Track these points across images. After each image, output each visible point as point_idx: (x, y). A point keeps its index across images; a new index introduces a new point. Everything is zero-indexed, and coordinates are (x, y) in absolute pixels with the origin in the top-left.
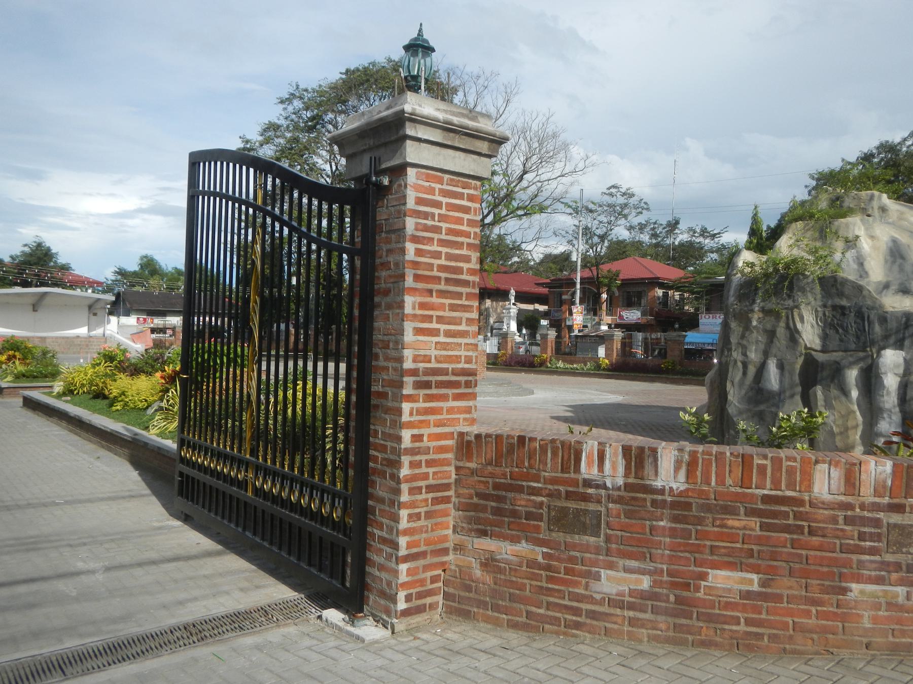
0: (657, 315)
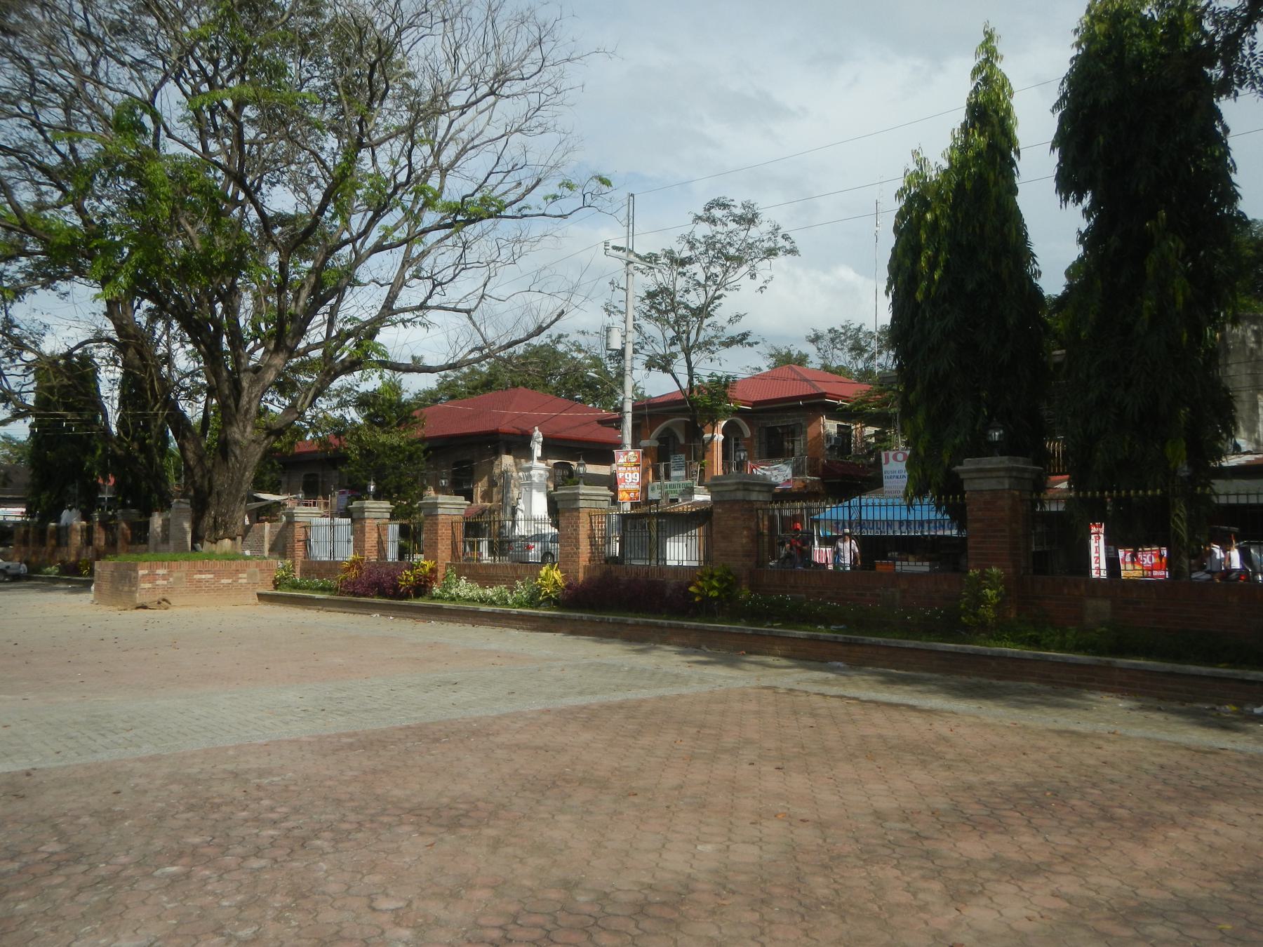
0: (826, 473)
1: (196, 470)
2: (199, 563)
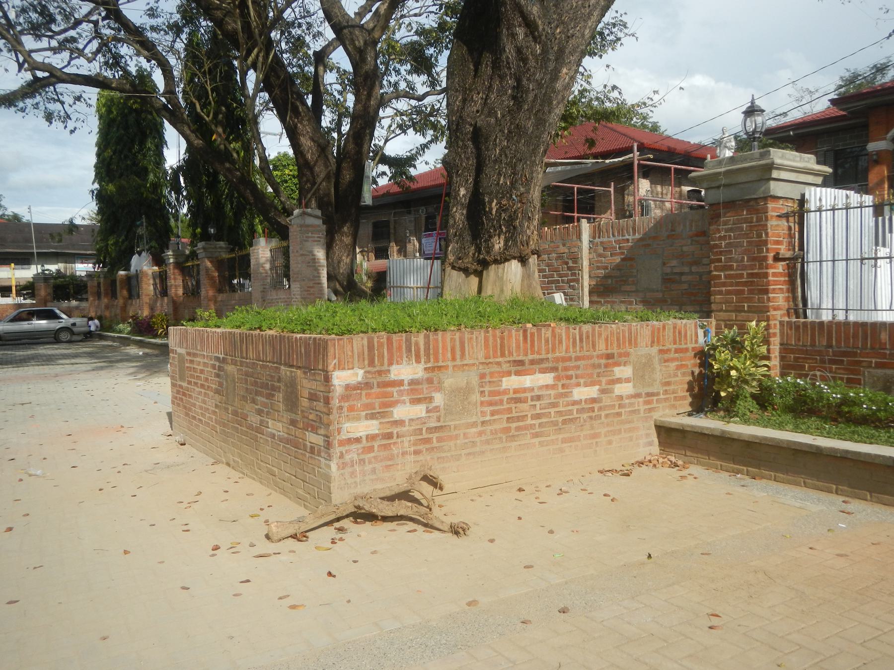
1: (317, 169)
2: (515, 334)
